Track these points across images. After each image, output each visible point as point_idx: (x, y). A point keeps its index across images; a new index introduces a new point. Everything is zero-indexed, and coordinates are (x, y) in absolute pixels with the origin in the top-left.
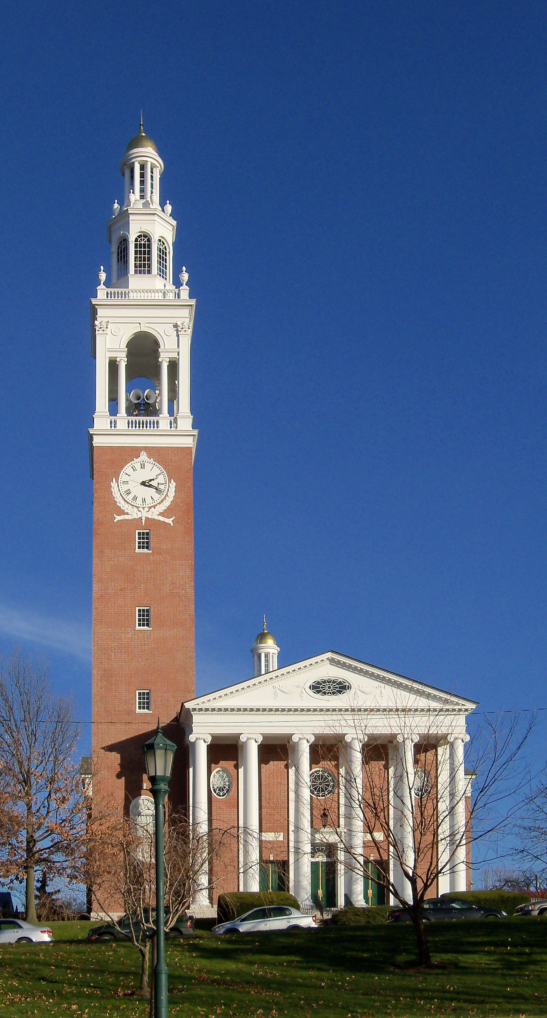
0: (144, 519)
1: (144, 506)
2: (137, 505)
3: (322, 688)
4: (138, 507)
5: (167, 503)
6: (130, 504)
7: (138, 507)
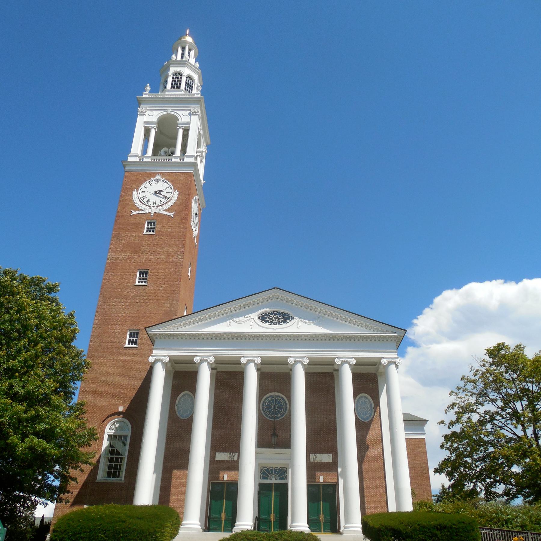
0: (153, 213)
1: (154, 205)
2: (149, 205)
3: (269, 318)
4: (149, 206)
5: (171, 204)
6: (144, 204)
7: (149, 206)
